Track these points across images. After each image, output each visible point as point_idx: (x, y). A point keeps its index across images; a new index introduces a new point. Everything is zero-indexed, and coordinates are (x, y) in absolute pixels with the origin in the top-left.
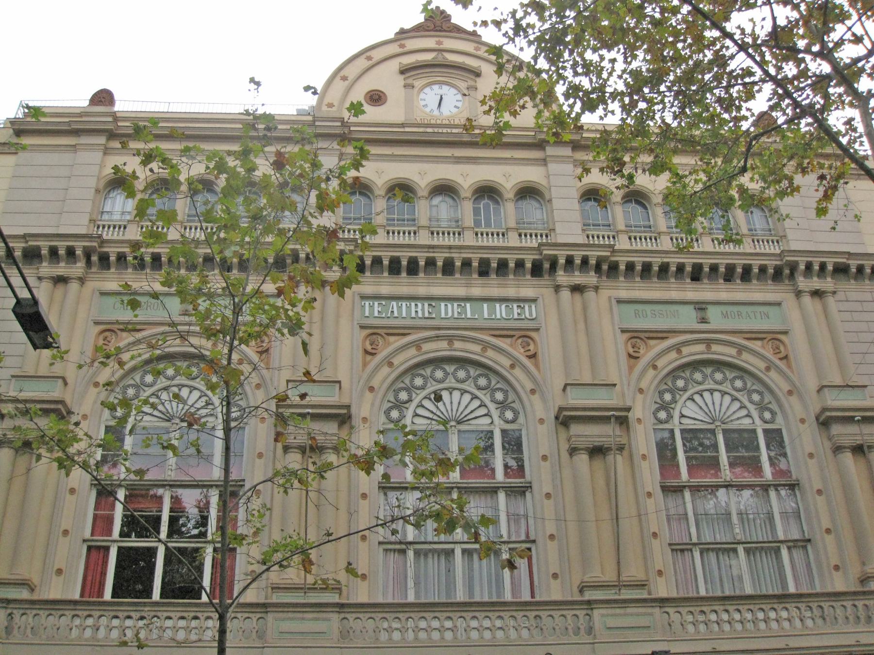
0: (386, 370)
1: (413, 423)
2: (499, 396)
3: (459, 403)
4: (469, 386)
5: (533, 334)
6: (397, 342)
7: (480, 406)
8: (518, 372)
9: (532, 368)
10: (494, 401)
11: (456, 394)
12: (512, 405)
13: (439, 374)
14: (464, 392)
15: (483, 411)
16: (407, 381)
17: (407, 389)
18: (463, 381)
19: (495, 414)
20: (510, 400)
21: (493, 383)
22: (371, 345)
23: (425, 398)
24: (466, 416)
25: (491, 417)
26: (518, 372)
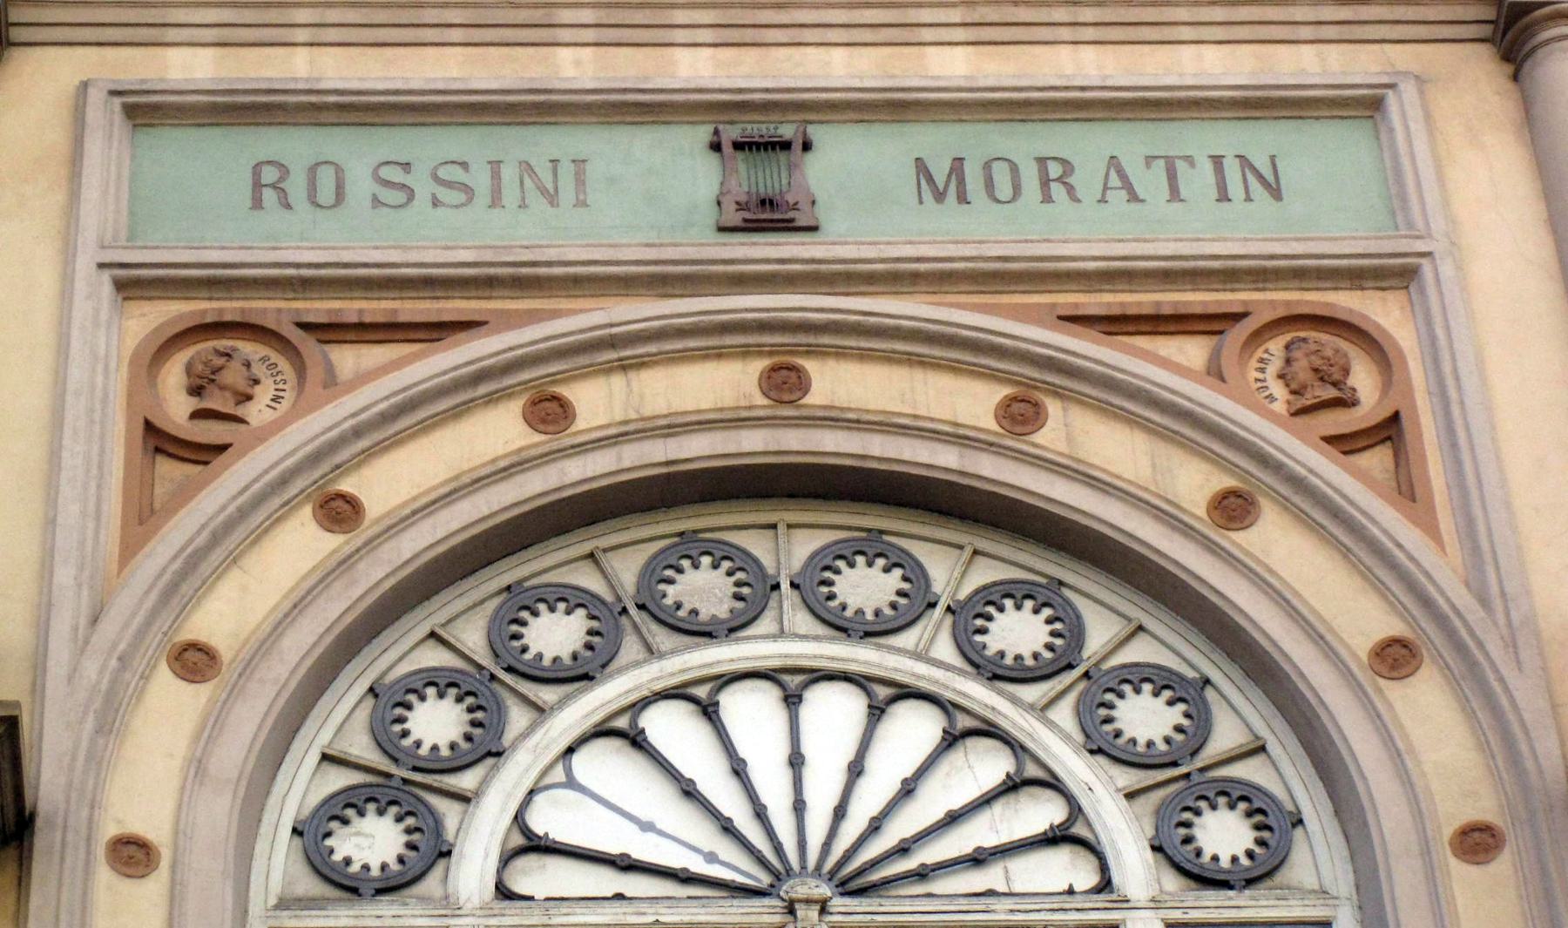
0: (301, 544)
1: (504, 892)
2: (1146, 718)
3: (856, 770)
4: (923, 652)
5: (1382, 311)
6: (376, 376)
7: (1012, 786)
8: (1275, 539)
9: (1387, 518)
10: (1103, 745)
11: (833, 714)
12: (1238, 771)
13: (703, 588)
14: (884, 697)
15: (1041, 813)
16: (473, 637)
17: (473, 689)
18: (874, 631)
19: (1125, 833)
20: (1225, 736)
21: (1099, 632)
22: (196, 391)
23: (602, 731)
24: (903, 849)
25: (1090, 847)
26: (1275, 539)
